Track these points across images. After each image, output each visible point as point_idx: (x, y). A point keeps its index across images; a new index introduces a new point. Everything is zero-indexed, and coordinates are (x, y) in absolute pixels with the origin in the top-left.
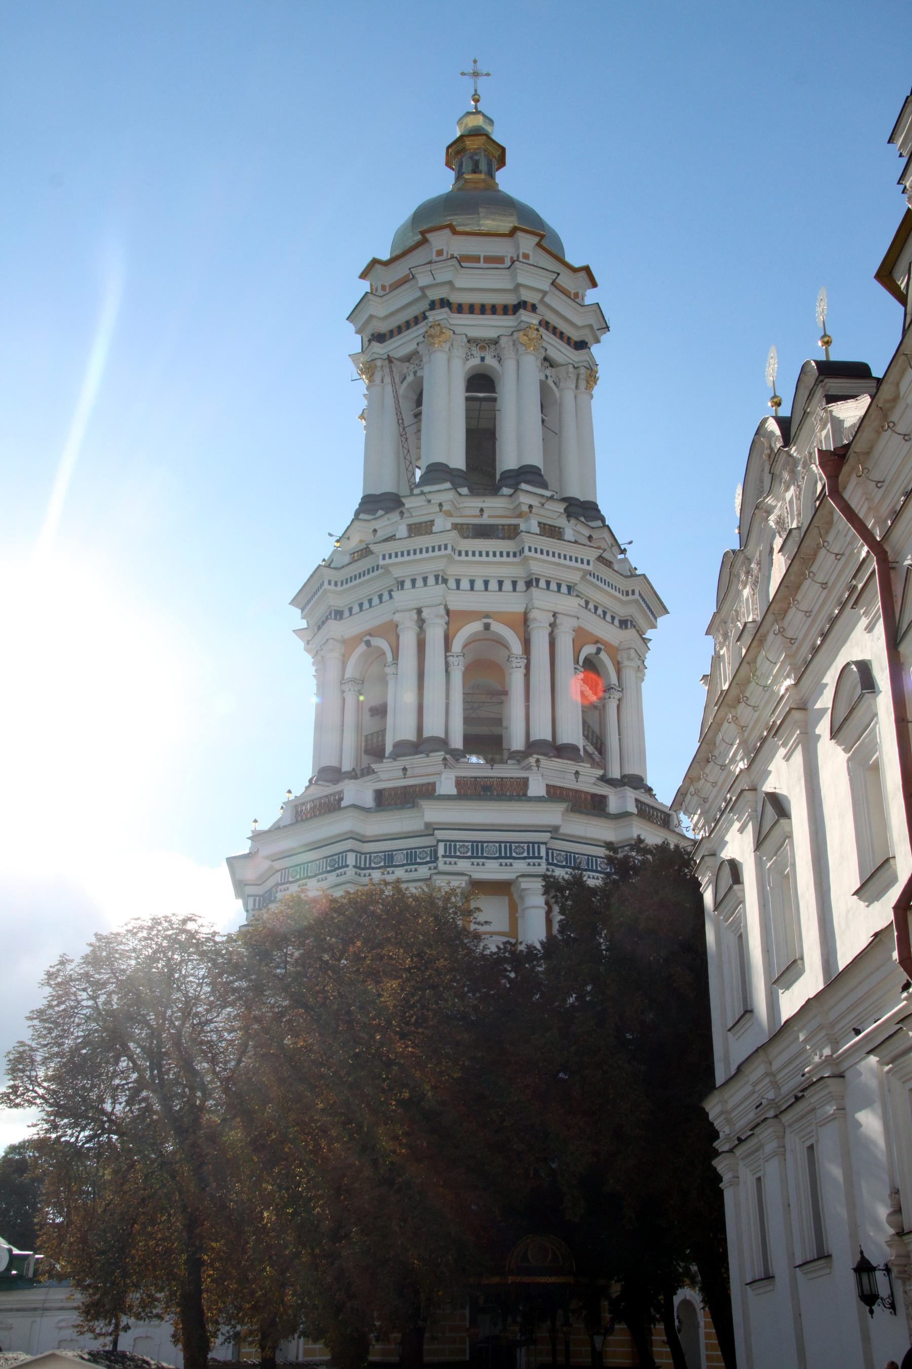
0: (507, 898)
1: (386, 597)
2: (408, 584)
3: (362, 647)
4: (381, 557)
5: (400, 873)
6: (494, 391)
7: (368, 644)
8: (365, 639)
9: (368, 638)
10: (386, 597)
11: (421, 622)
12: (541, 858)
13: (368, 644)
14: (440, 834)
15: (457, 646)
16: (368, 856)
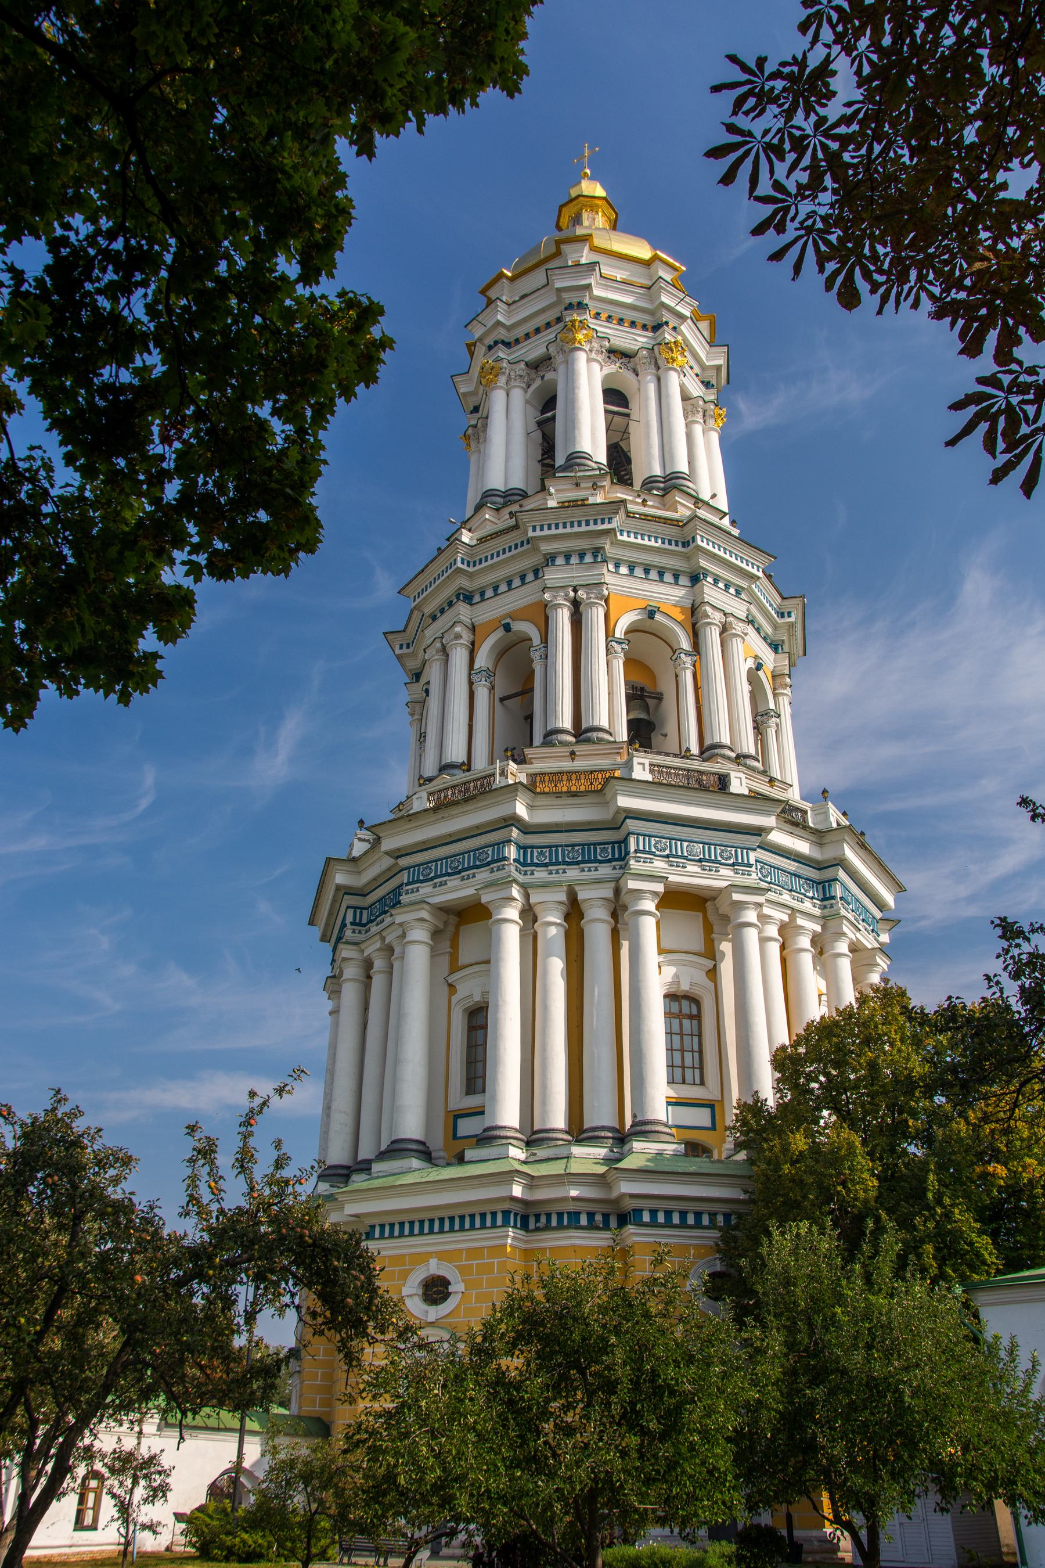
0: (700, 914)
1: (530, 577)
2: (560, 561)
3: (500, 633)
4: (530, 529)
5: (573, 873)
6: (627, 406)
7: (507, 628)
8: (503, 622)
9: (508, 620)
10: (530, 577)
11: (576, 604)
12: (751, 866)
13: (507, 628)
14: (631, 824)
15: (619, 633)
16: (529, 850)
